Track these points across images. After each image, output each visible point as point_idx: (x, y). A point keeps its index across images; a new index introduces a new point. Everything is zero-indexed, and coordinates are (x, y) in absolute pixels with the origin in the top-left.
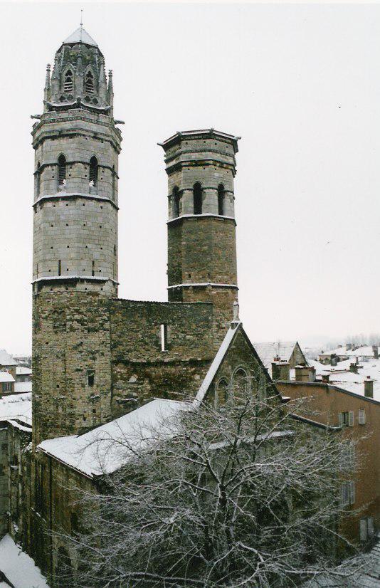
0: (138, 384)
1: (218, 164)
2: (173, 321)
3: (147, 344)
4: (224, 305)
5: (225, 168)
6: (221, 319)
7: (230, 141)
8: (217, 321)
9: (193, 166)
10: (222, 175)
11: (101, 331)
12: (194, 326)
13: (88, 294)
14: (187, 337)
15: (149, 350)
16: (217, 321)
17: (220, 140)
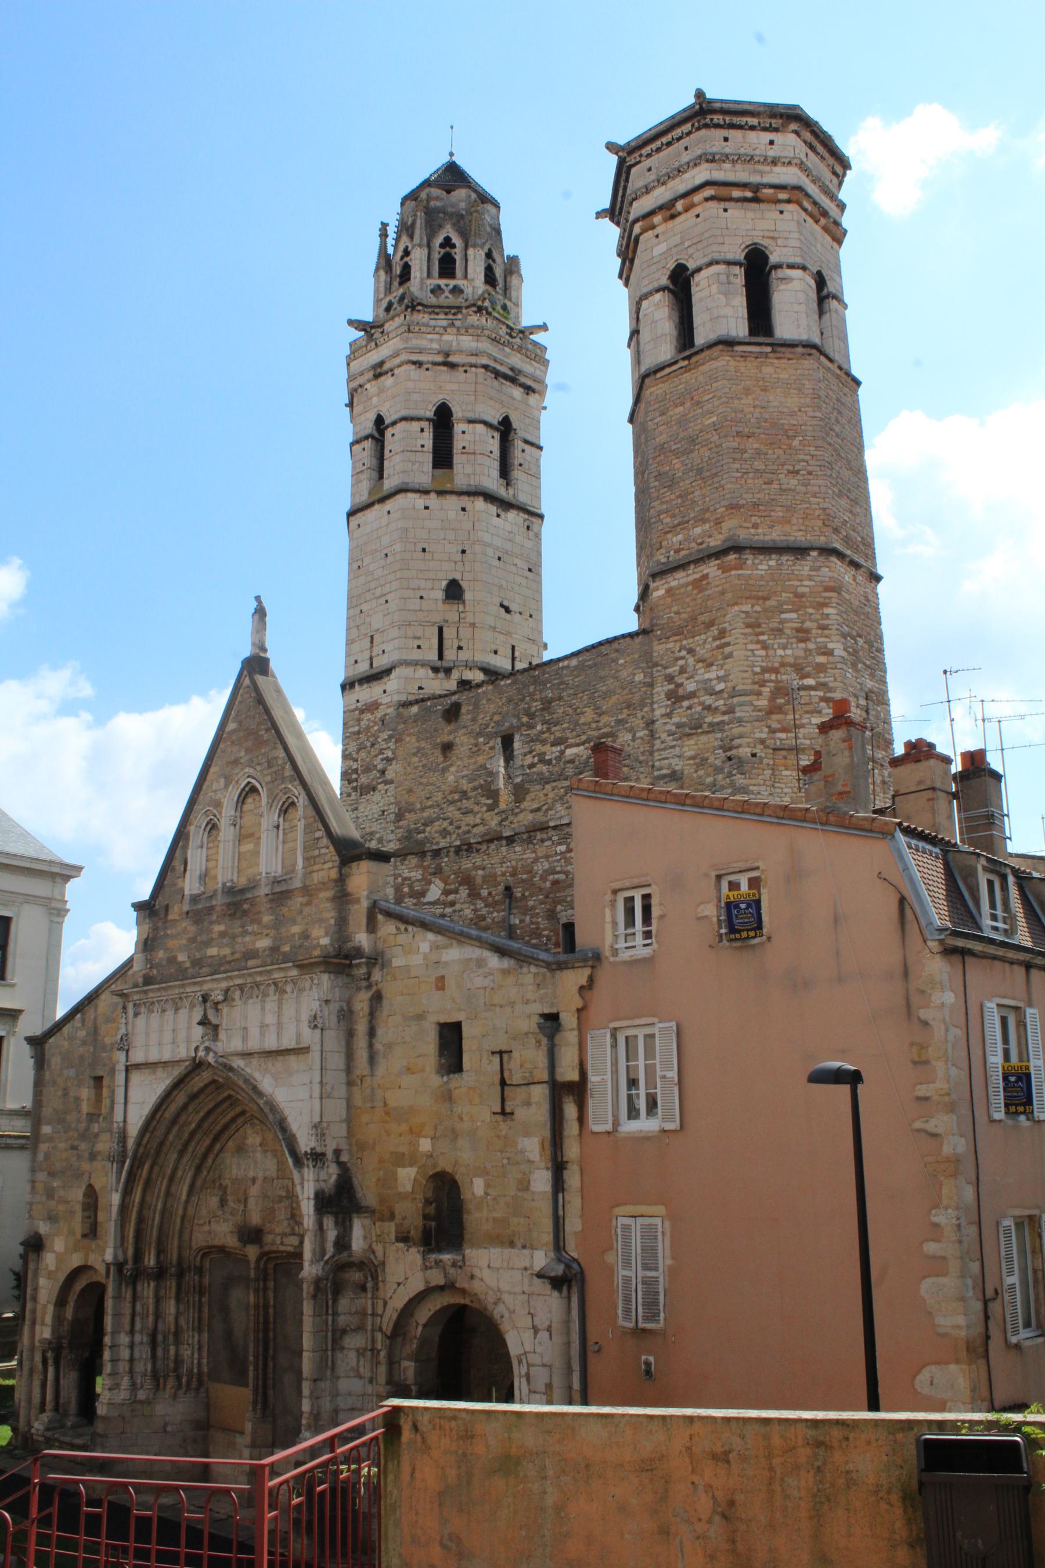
0: (445, 904)
1: (657, 219)
2: (531, 716)
3: (464, 794)
4: (694, 619)
5: (687, 210)
6: (682, 670)
7: (687, 127)
8: (670, 679)
9: (631, 269)
10: (677, 239)
11: (380, 787)
12: (589, 715)
13: (362, 712)
14: (569, 752)
15: (471, 811)
16: (670, 679)
17: (658, 150)
